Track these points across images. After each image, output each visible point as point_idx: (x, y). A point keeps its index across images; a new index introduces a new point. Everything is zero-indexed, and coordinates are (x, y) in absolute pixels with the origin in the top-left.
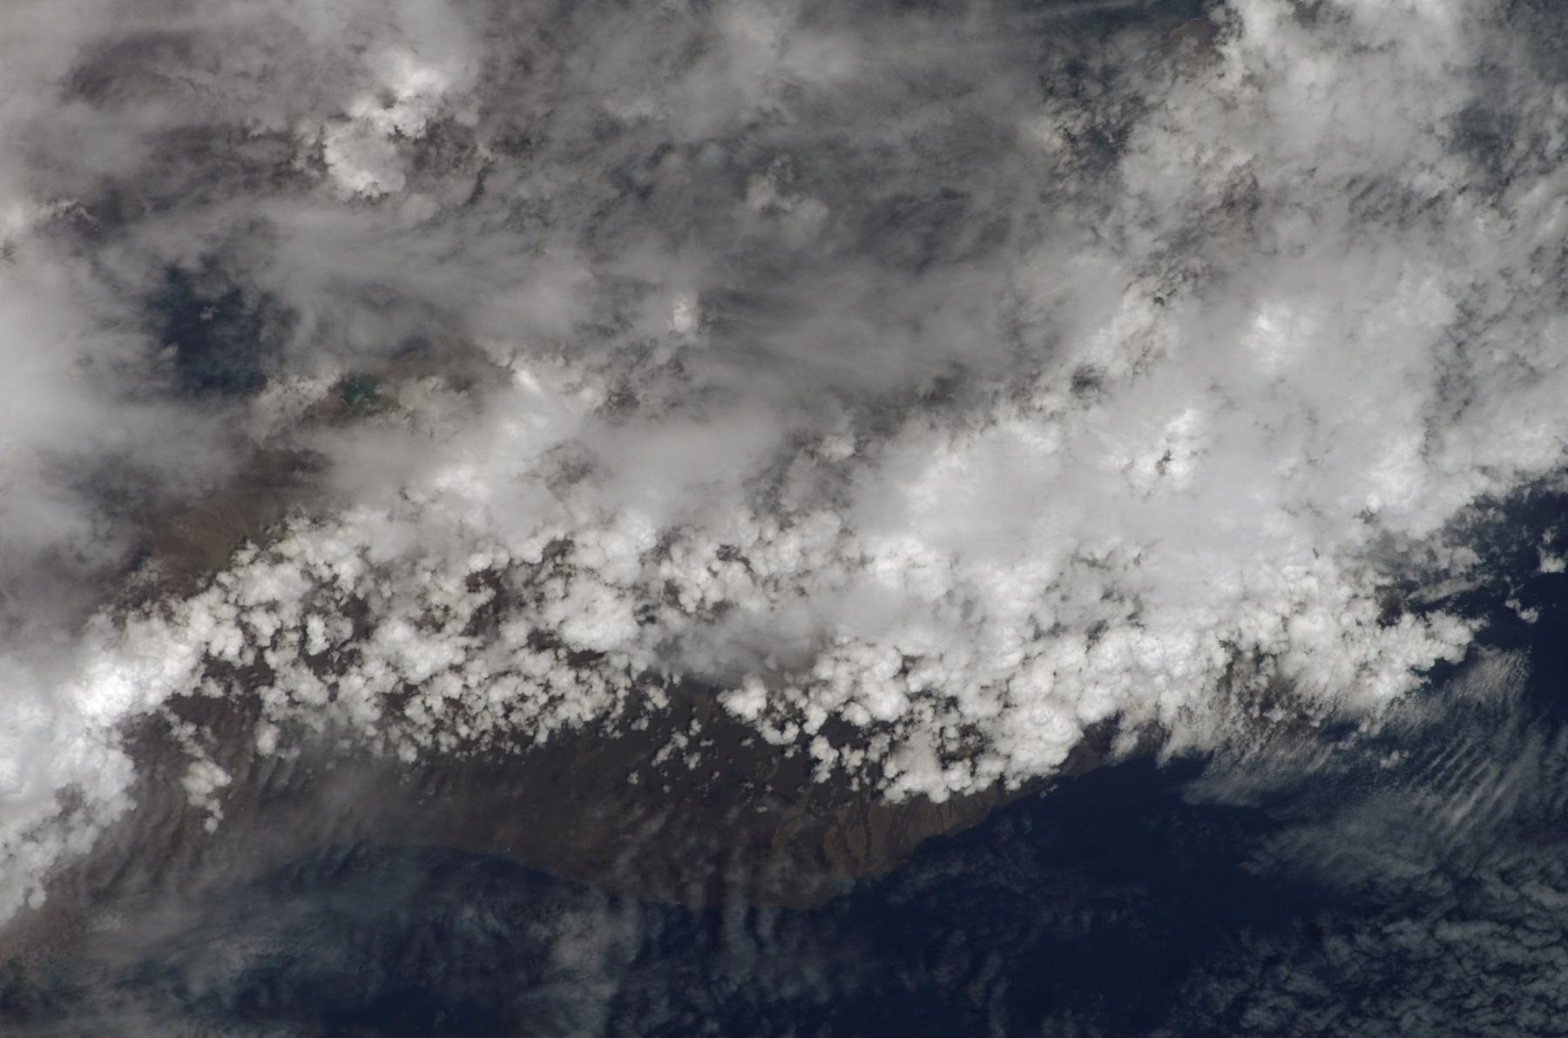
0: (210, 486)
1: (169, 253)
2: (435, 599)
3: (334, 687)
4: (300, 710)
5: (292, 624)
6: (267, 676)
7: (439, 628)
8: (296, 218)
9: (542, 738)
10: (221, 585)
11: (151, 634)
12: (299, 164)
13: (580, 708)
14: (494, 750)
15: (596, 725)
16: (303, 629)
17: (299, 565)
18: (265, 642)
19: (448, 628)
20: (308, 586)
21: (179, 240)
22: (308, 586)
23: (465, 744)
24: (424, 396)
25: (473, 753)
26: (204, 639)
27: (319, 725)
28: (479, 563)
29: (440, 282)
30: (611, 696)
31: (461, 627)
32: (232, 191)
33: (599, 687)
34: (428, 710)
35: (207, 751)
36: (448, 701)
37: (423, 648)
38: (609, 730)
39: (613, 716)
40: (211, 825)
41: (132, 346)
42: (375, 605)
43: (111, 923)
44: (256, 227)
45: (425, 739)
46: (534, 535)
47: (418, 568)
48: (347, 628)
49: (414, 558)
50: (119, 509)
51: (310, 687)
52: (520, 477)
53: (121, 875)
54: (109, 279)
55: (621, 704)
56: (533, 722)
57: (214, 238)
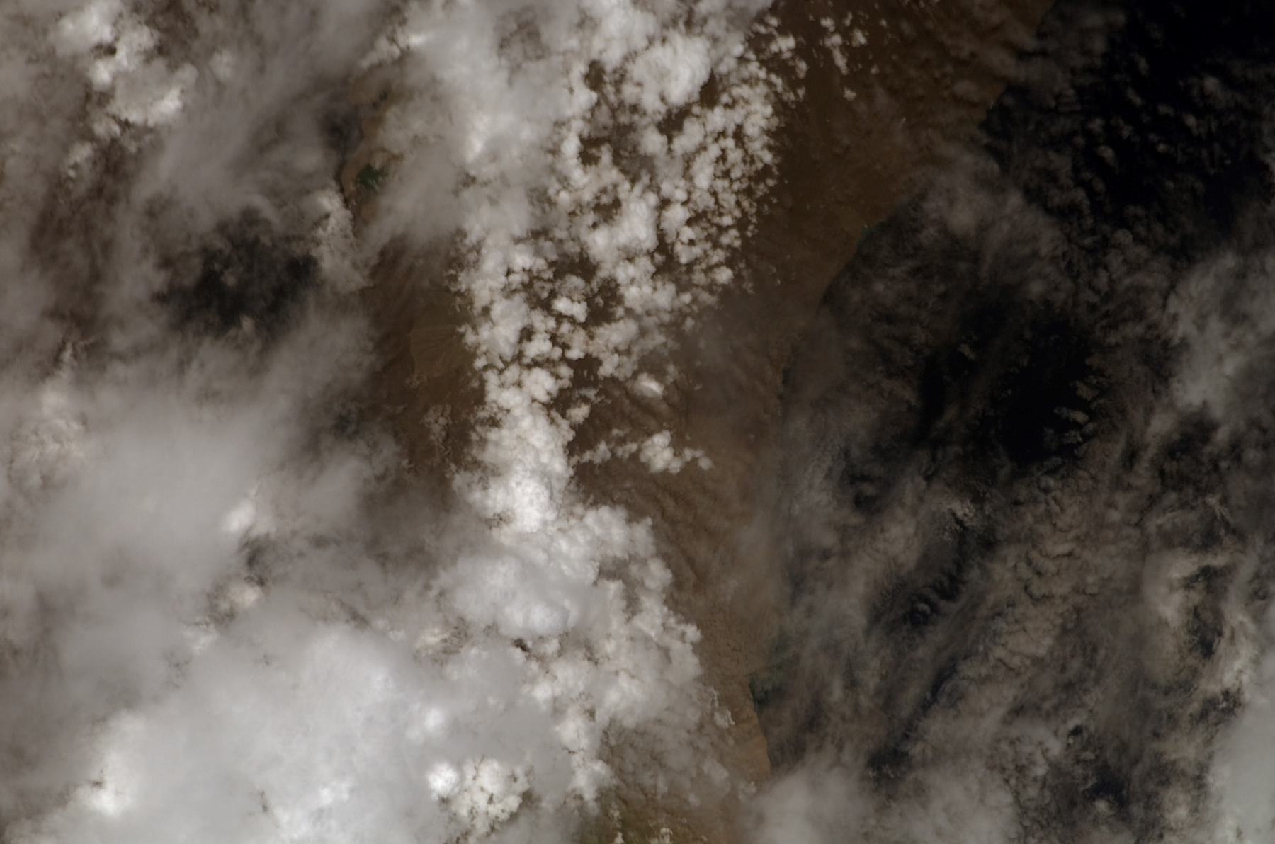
0: (370, 345)
1: (141, 292)
2: (587, 196)
3: (629, 312)
4: (636, 349)
5: (551, 323)
6: (588, 364)
7: (617, 203)
8: (160, 175)
9: (768, 157)
10: (486, 368)
11: (497, 444)
12: (132, 148)
13: (758, 115)
14: (760, 202)
15: (781, 108)
16: (560, 318)
17: (498, 297)
18: (557, 353)
19: (622, 196)
20: (519, 298)
21: (135, 279)
22: (519, 298)
23: (741, 224)
24: (398, 130)
25: (754, 220)
26: (527, 402)
27: (658, 339)
28: (571, 146)
29: (282, 77)
30: (761, 84)
31: (627, 185)
32: (109, 216)
33: (744, 91)
34: (692, 243)
35: (633, 440)
36: (689, 223)
37: (626, 225)
38: (792, 97)
39: (780, 89)
40: (705, 464)
41: (214, 357)
42: (572, 248)
43: (730, 586)
44: (155, 210)
45: (718, 256)
46: (571, 90)
47: (553, 197)
48: (575, 281)
49: (541, 198)
50: (352, 428)
51: (616, 333)
52: (510, 82)
53: (691, 561)
54: (137, 352)
55: (773, 78)
56: (749, 159)
57: (145, 251)
